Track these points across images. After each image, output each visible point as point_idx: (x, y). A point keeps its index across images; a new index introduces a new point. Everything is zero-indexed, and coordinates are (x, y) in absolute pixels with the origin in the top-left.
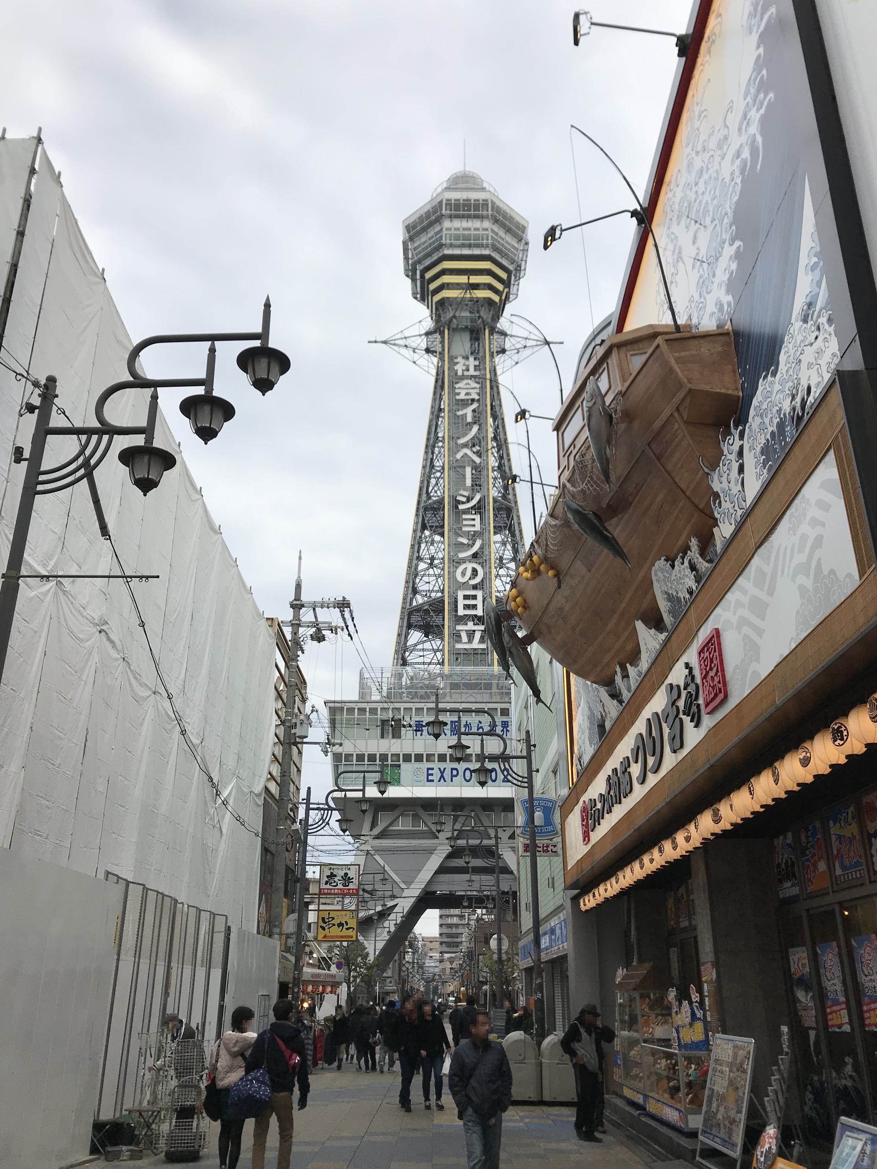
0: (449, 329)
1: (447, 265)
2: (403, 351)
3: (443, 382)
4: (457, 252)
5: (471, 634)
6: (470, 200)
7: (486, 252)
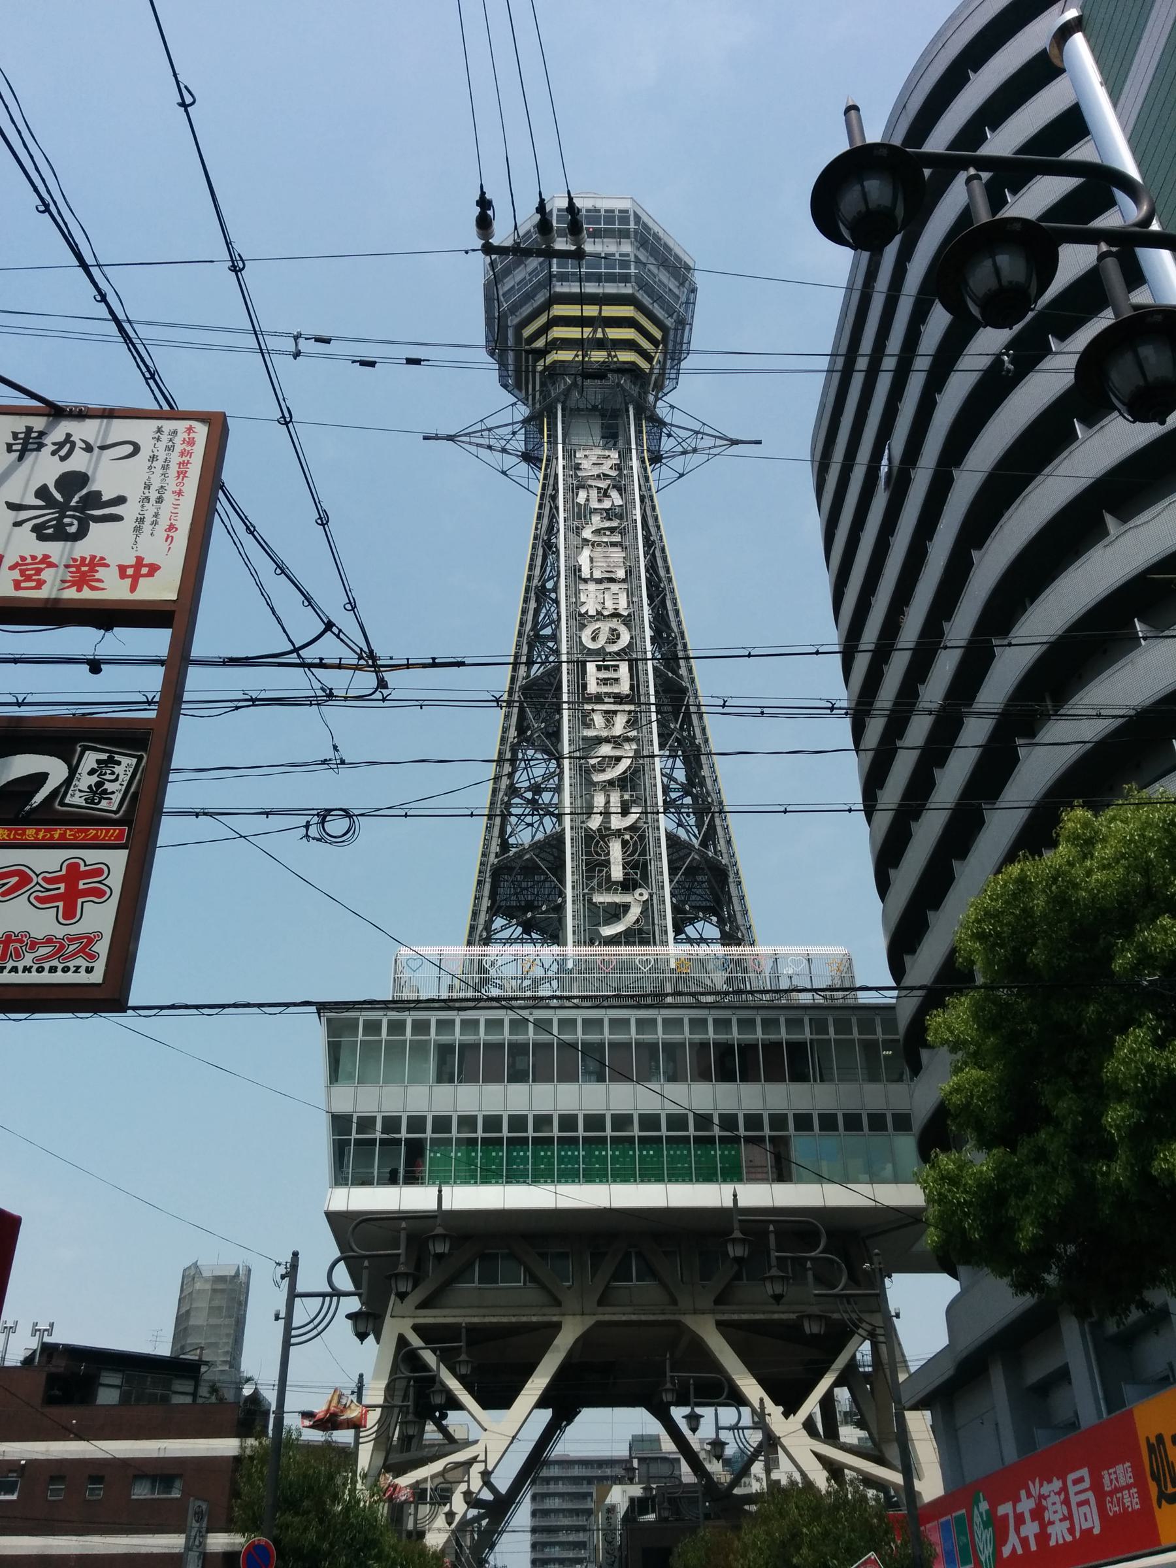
0: (563, 410)
1: (559, 310)
2: (484, 453)
3: (556, 489)
6: (599, 211)
7: (627, 289)
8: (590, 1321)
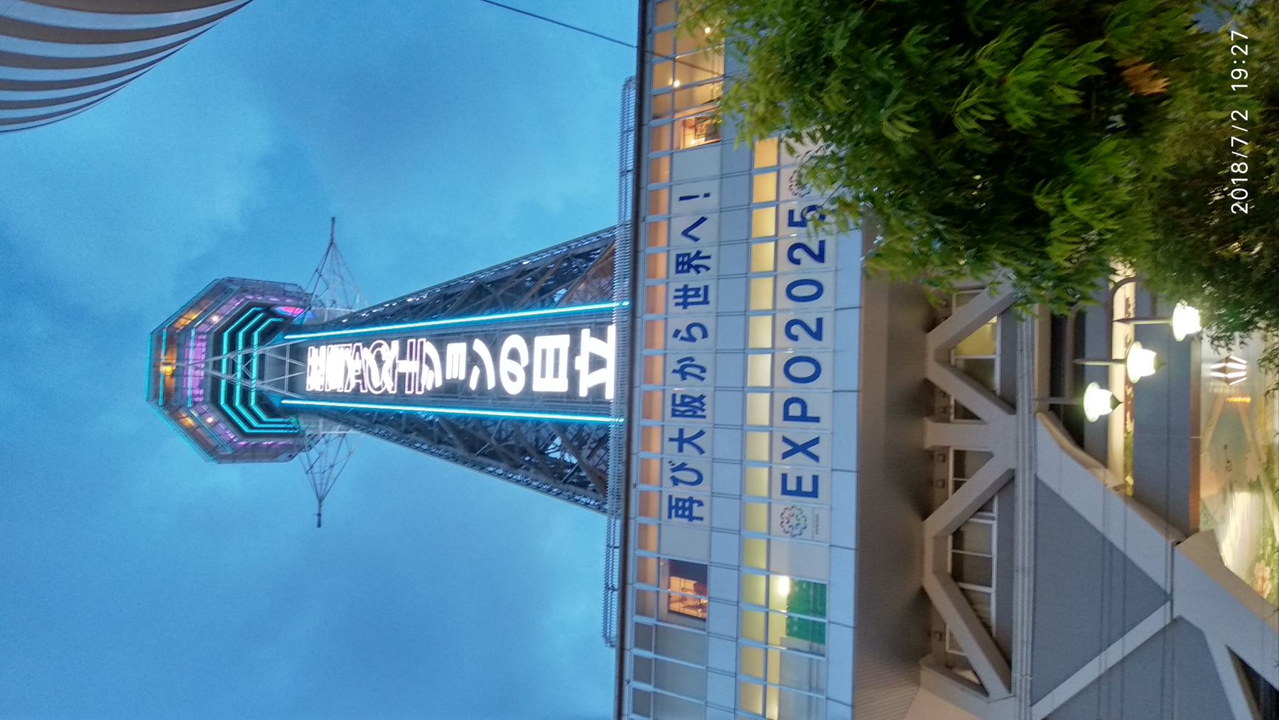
5: (597, 363)
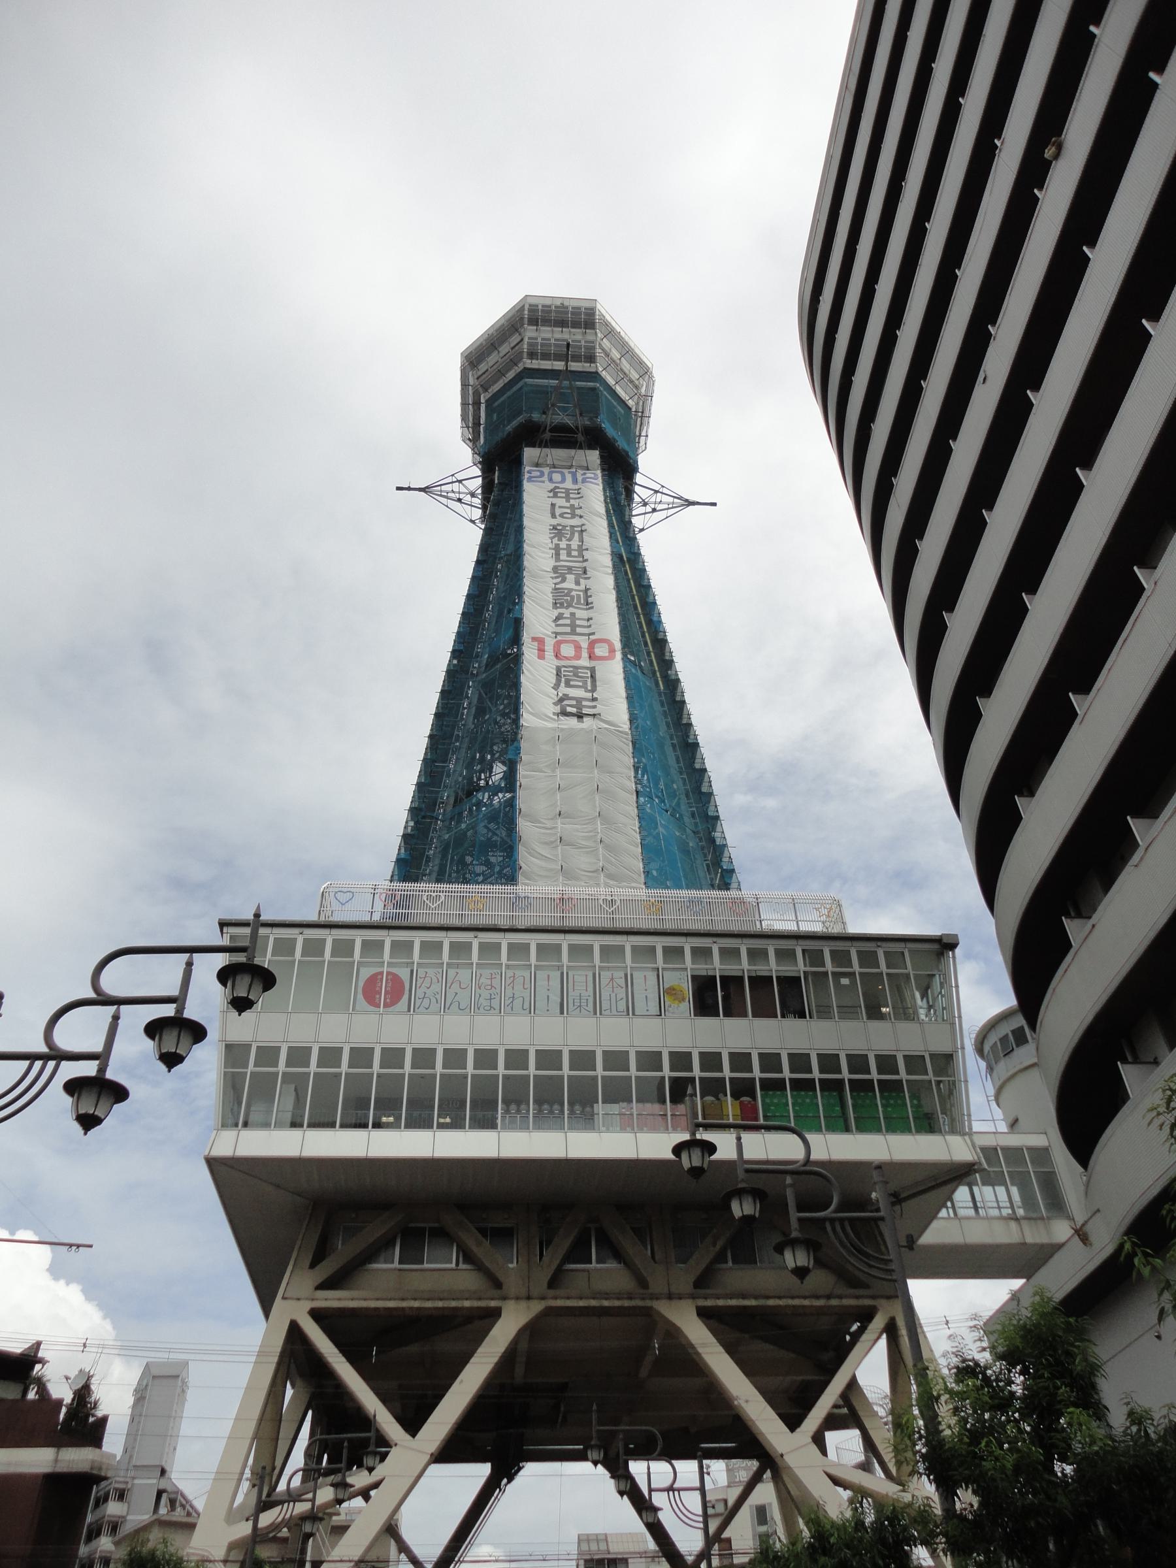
4: (546, 365)
8: (537, 1307)
